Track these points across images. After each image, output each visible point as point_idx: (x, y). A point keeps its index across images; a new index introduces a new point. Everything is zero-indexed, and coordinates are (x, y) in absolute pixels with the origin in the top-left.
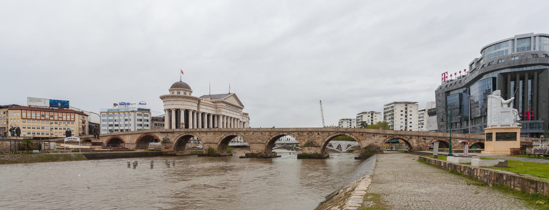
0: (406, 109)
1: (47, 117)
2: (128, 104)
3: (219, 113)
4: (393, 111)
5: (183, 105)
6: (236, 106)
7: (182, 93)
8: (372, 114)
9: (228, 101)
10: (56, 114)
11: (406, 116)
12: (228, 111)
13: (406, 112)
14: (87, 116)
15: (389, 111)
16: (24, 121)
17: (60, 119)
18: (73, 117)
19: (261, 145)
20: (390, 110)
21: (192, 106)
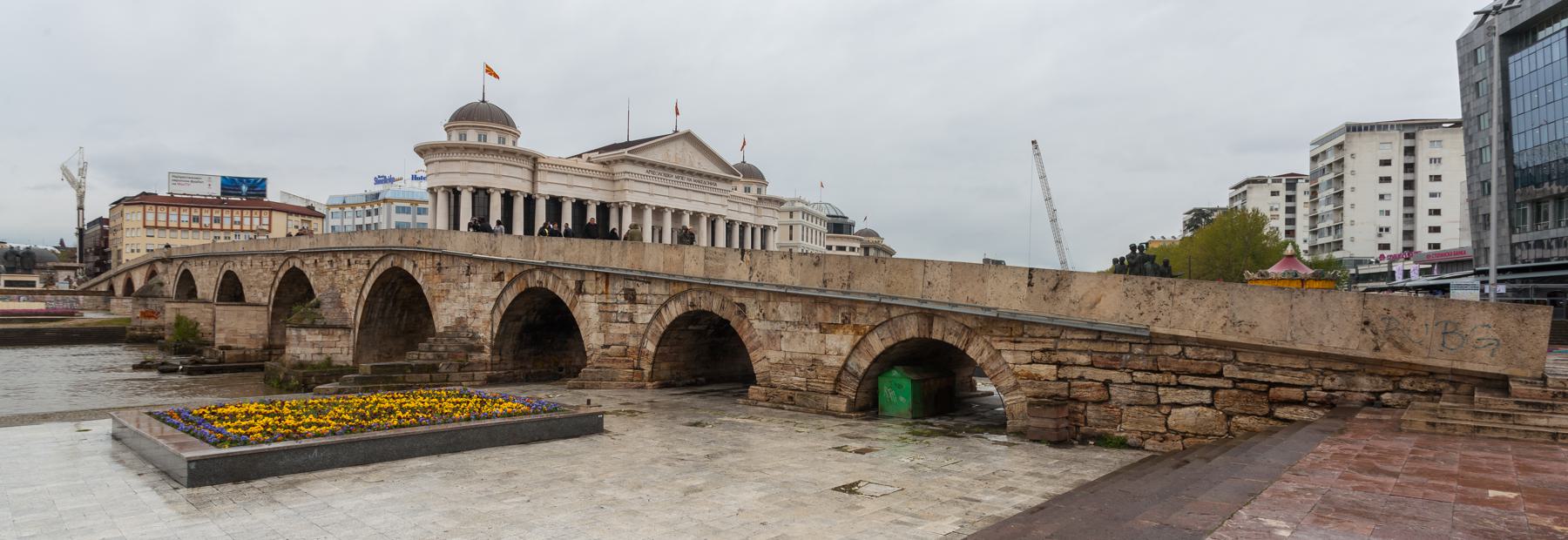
0: (1410, 151)
1: (206, 221)
2: (392, 180)
3: (619, 198)
4: (1340, 162)
5: (467, 175)
6: (717, 178)
7: (472, 138)
8: (1291, 185)
9: (656, 156)
10: (227, 214)
11: (1409, 185)
12: (665, 191)
13: (1409, 168)
14: (322, 217)
15: (1331, 161)
16: (150, 232)
17: (237, 227)
18: (265, 221)
19: (251, 311)
20: (1331, 159)
21: (517, 180)
